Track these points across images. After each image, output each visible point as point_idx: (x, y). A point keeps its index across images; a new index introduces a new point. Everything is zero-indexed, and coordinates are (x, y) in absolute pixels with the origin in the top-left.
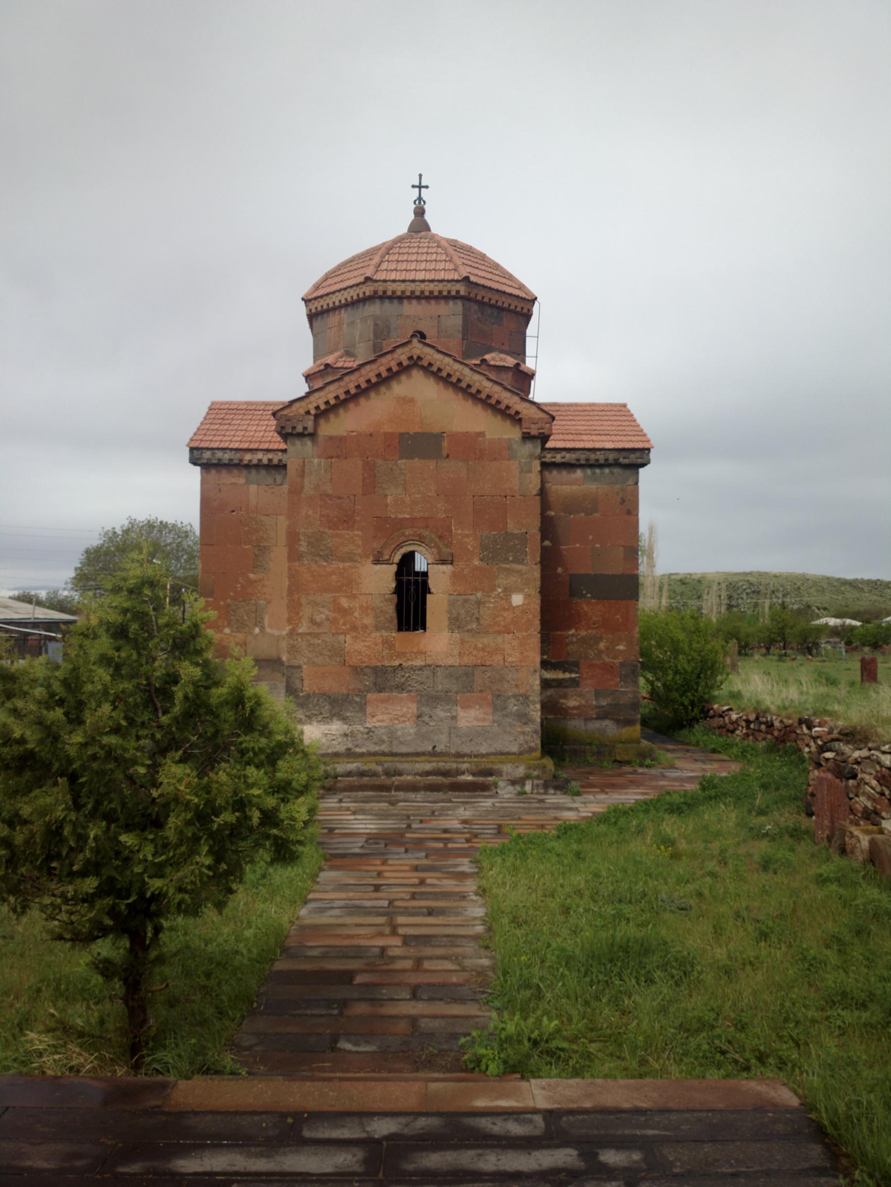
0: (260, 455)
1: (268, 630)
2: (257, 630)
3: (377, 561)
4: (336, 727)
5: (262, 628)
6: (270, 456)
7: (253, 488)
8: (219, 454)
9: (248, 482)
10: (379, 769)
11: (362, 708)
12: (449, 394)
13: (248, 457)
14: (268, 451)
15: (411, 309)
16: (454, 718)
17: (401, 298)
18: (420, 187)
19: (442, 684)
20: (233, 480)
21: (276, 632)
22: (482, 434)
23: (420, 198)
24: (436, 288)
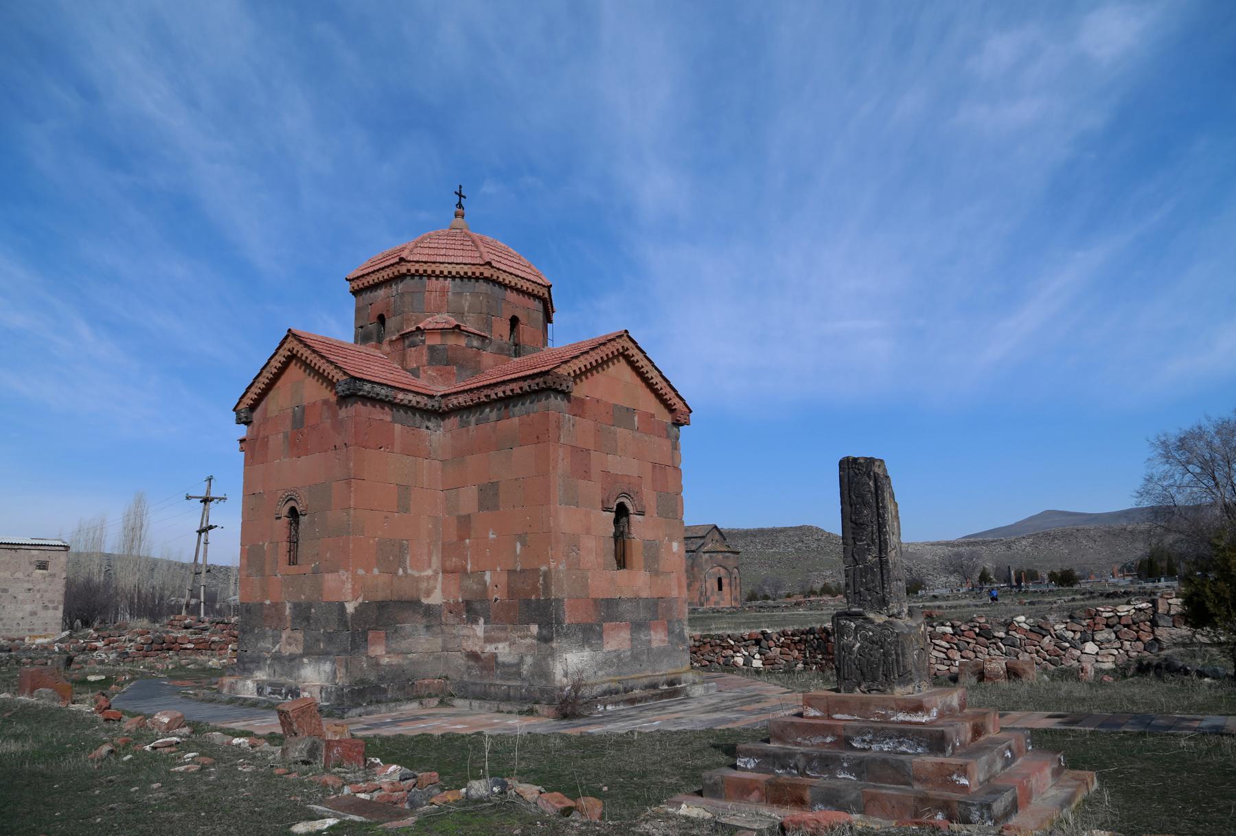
0: (410, 397)
1: (409, 571)
2: (401, 571)
3: (606, 509)
4: (586, 654)
5: (405, 571)
6: (419, 398)
7: (398, 427)
8: (378, 389)
9: (394, 421)
10: (621, 687)
11: (601, 638)
12: (638, 381)
13: (400, 396)
14: (418, 393)
15: (511, 296)
16: (650, 641)
17: (506, 286)
18: (460, 196)
19: (643, 615)
20: (381, 417)
21: (416, 574)
22: (653, 416)
23: (460, 205)
24: (531, 287)
